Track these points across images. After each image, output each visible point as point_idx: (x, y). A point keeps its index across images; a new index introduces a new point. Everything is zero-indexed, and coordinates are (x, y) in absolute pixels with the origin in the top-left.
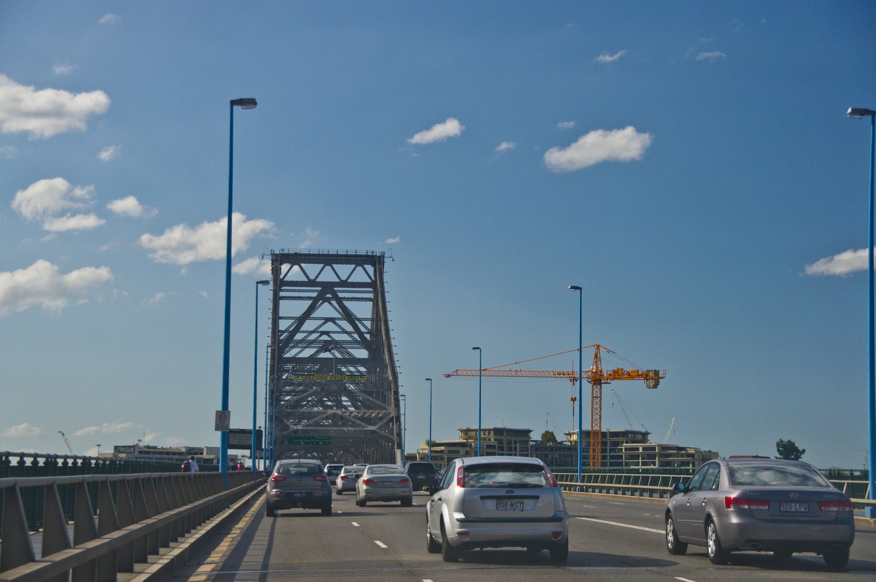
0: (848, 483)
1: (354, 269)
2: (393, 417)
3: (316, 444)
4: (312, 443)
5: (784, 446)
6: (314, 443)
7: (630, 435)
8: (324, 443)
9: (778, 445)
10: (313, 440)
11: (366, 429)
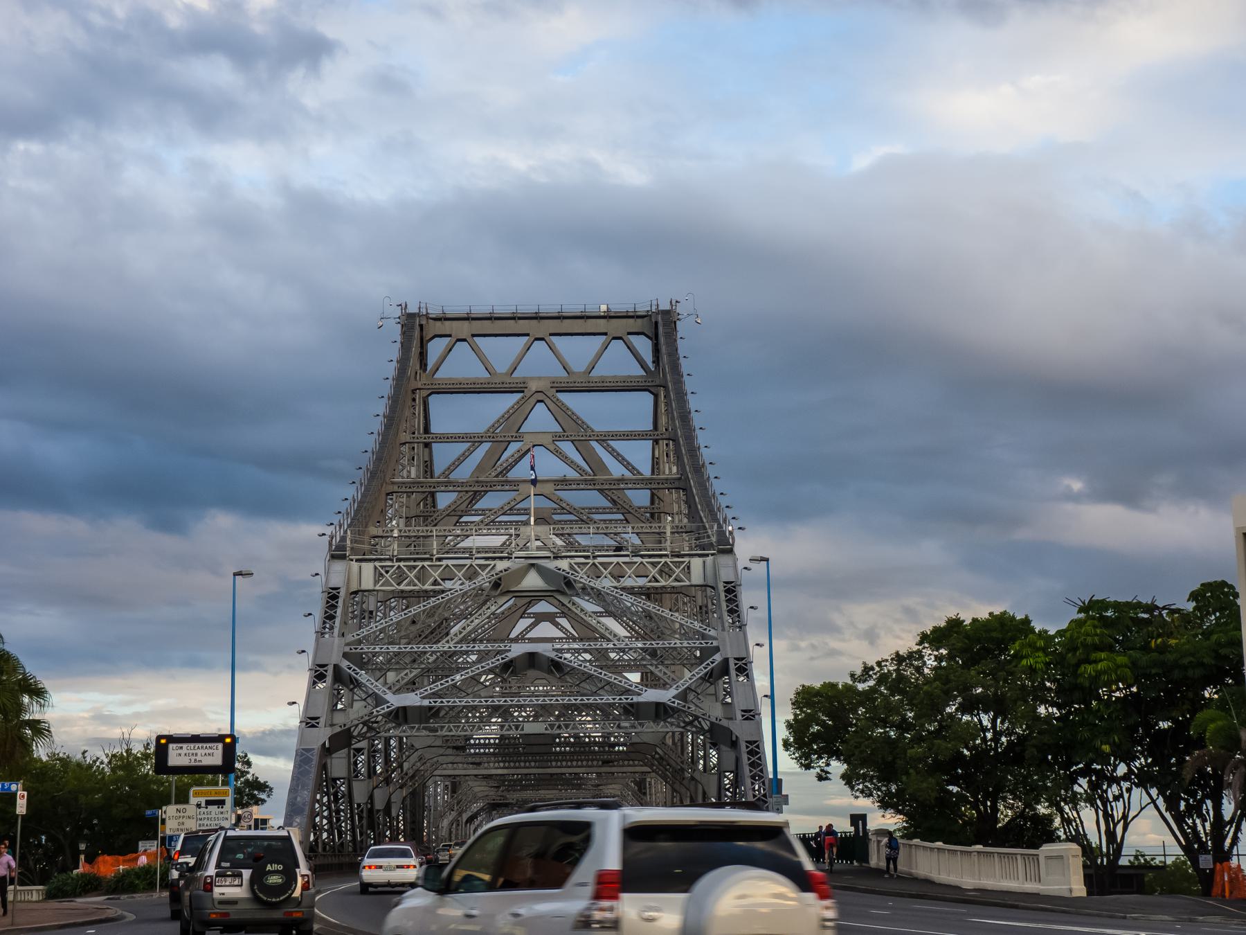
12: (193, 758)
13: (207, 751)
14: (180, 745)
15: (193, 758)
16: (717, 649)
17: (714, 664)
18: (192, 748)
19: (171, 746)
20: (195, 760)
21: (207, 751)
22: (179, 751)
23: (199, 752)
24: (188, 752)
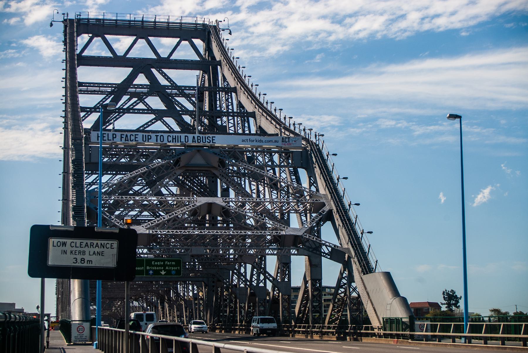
0: (454, 324)
1: (178, 44)
2: (331, 211)
3: (153, 274)
4: (147, 272)
5: (448, 294)
6: (151, 272)
7: (327, 289)
8: (169, 272)
9: (444, 293)
10: (148, 268)
11: (283, 233)
12: (79, 257)
13: (97, 250)
14: (61, 240)
15: (79, 257)
16: (323, 205)
17: (324, 213)
18: (78, 245)
19: (52, 241)
20: (83, 260)
21: (97, 250)
22: (64, 248)
23: (87, 249)
24: (74, 249)
